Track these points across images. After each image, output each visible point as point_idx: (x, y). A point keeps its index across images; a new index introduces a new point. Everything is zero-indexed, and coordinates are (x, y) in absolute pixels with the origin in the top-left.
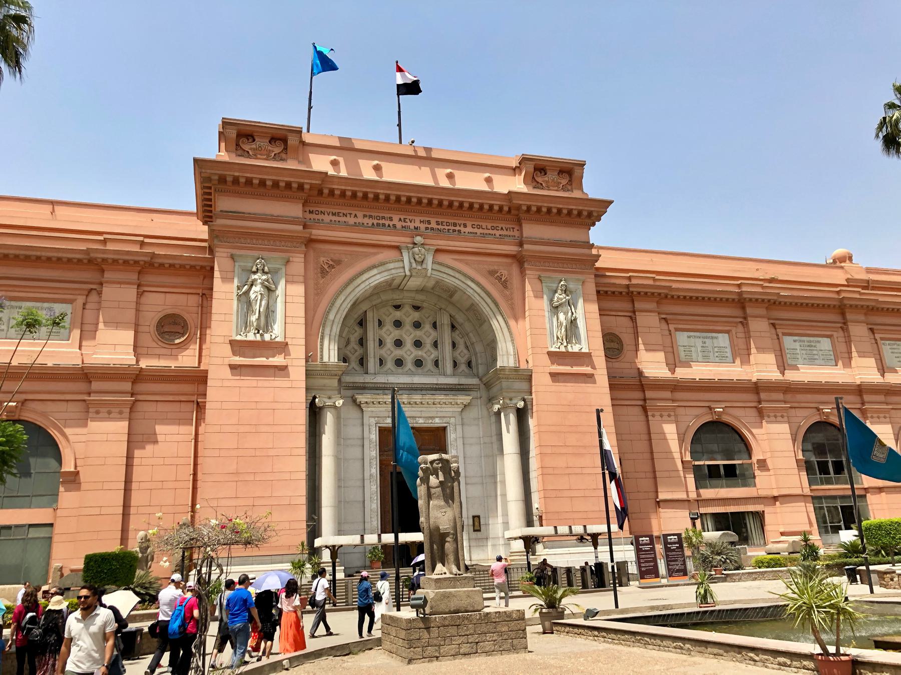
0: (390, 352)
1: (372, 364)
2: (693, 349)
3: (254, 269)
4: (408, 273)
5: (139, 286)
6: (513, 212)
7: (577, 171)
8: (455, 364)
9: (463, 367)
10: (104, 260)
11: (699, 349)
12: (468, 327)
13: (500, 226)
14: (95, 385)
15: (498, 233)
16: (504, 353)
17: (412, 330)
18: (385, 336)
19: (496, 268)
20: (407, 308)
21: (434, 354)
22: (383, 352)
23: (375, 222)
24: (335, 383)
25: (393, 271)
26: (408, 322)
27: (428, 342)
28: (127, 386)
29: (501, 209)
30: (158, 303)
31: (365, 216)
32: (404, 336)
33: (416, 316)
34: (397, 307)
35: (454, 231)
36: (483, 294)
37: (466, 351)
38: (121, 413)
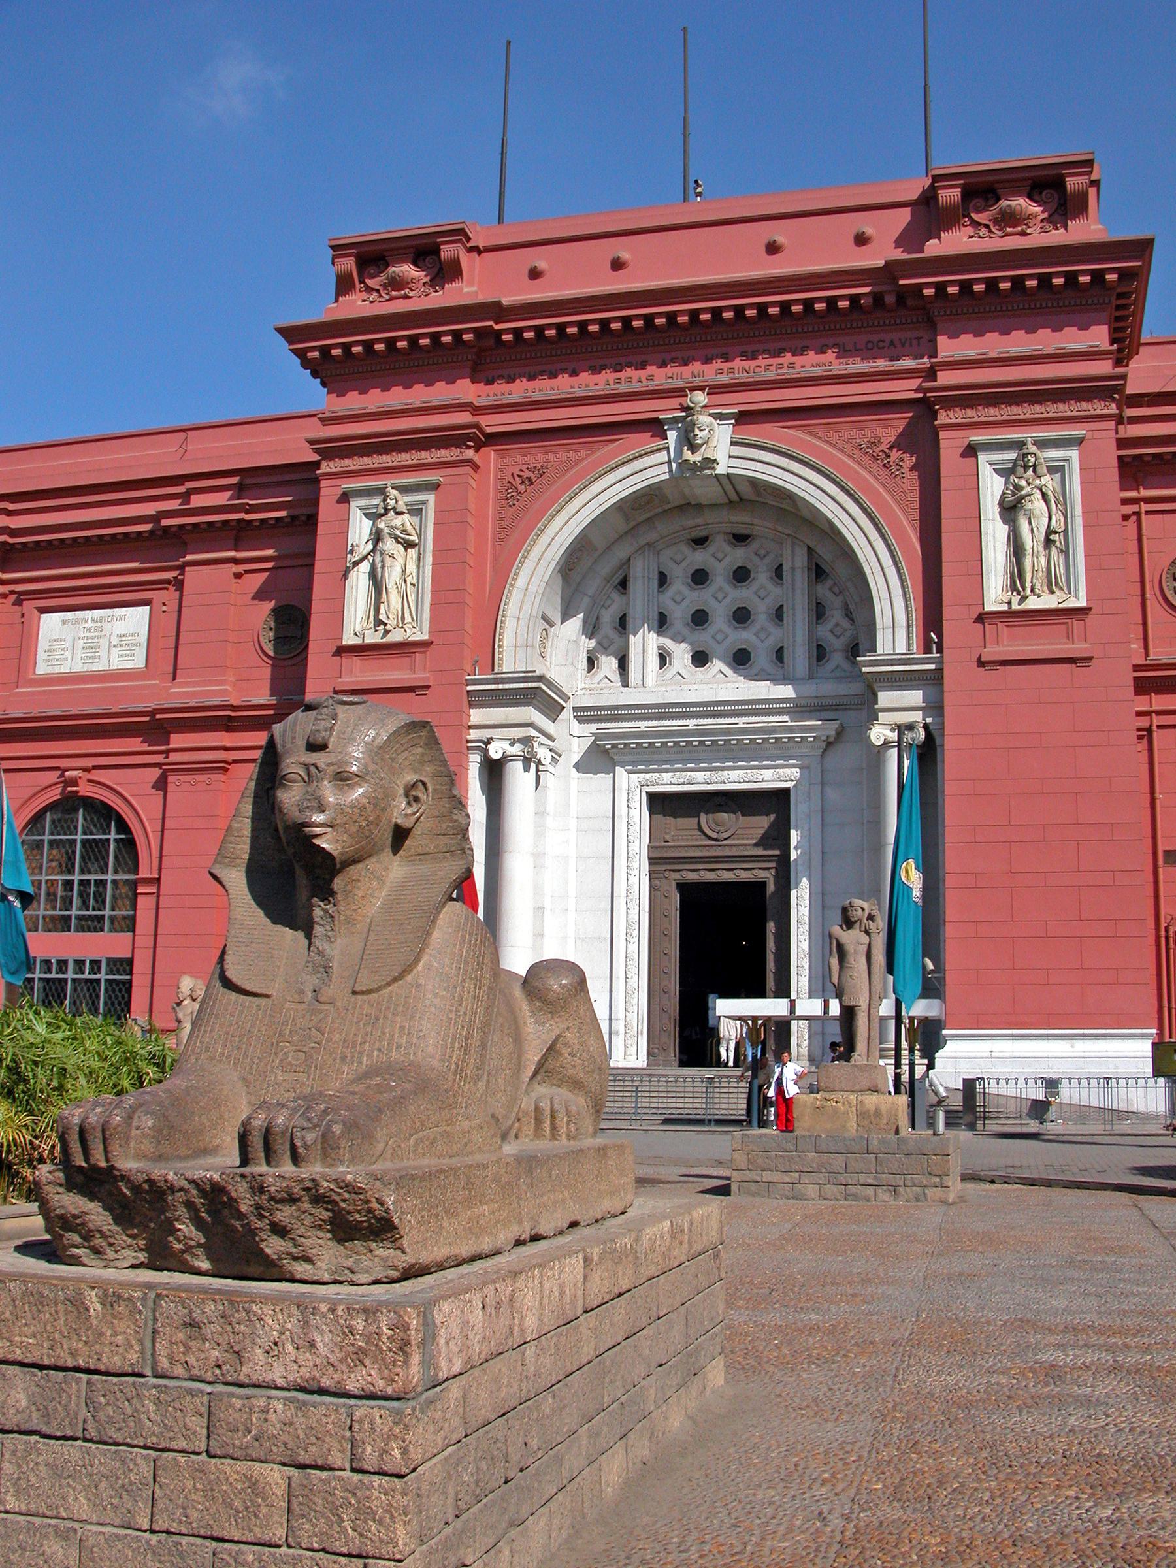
6: (910, 302)
8: (820, 653)
9: (837, 659)
10: (181, 527)
12: (841, 570)
13: (888, 337)
14: (177, 740)
16: (889, 623)
18: (671, 605)
20: (719, 544)
21: (775, 635)
27: (761, 611)
29: (877, 298)
32: (713, 603)
33: (739, 556)
34: (700, 542)
37: (845, 623)
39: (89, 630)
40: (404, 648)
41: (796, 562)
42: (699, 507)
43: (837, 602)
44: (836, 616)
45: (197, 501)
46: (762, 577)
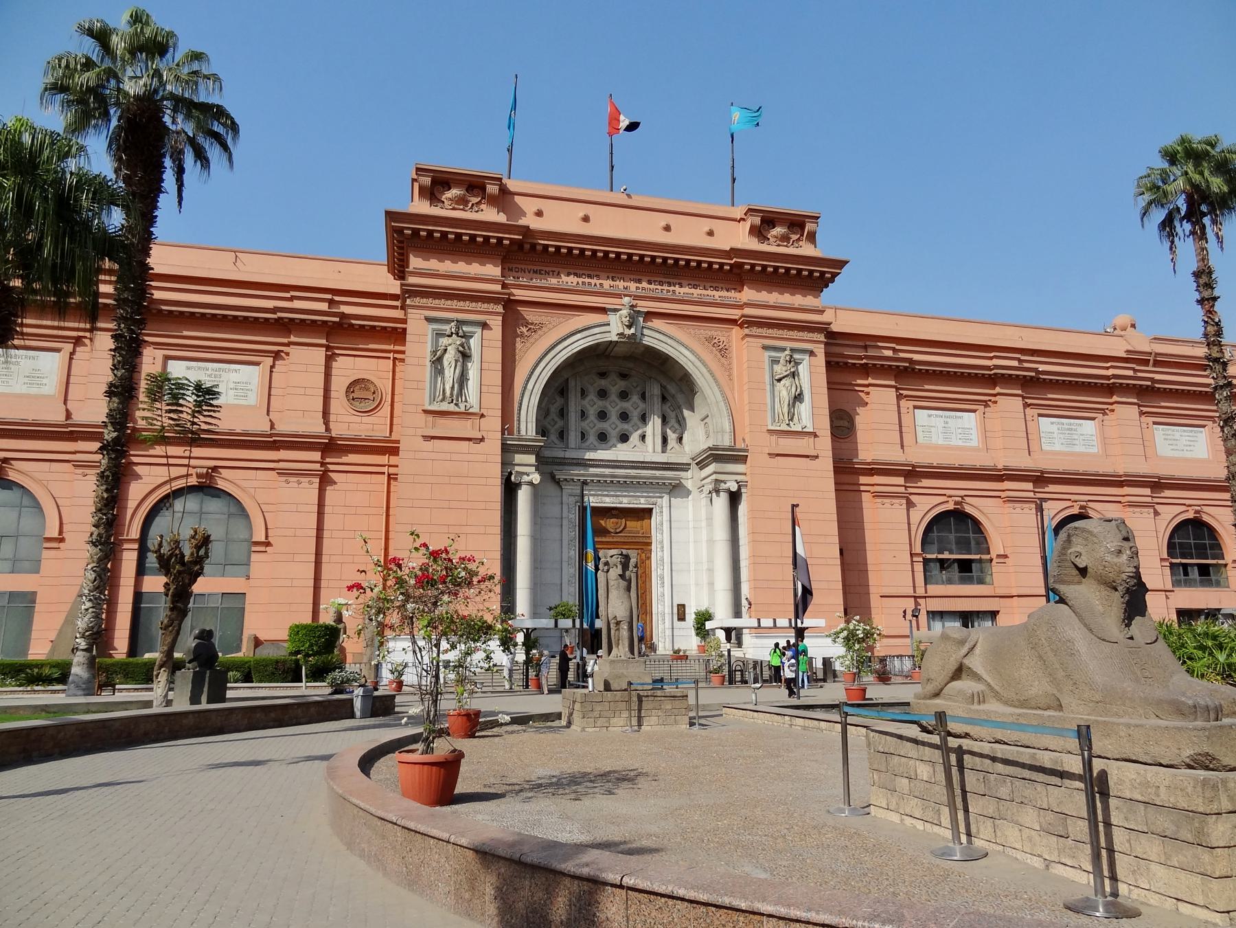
0: (593, 426)
1: (573, 437)
2: (933, 430)
3: (448, 333)
4: (615, 338)
5: (328, 348)
6: (735, 270)
7: (809, 227)
8: (665, 440)
11: (941, 430)
12: (680, 398)
15: (717, 294)
17: (617, 401)
19: (714, 333)
20: (613, 376)
22: (584, 424)
23: (580, 280)
24: (531, 459)
25: (598, 336)
26: (614, 391)
27: (635, 415)
28: (317, 456)
30: (348, 367)
31: (568, 274)
33: (622, 385)
34: (603, 375)
35: (668, 291)
36: (698, 364)
37: (677, 426)
38: (311, 483)
39: (210, 376)
40: (467, 414)
41: (656, 391)
42: (608, 357)
43: (673, 415)
44: (673, 422)
45: (297, 304)
46: (635, 398)
